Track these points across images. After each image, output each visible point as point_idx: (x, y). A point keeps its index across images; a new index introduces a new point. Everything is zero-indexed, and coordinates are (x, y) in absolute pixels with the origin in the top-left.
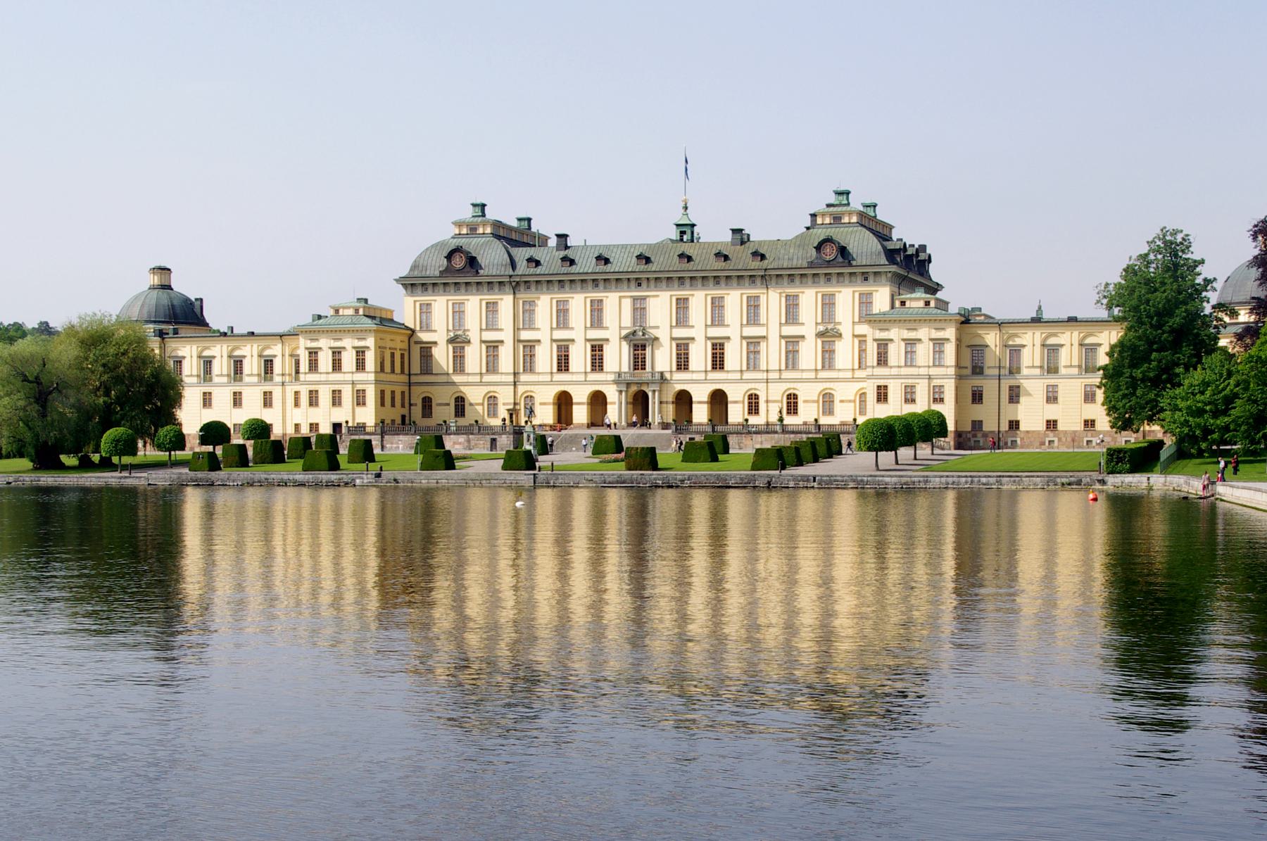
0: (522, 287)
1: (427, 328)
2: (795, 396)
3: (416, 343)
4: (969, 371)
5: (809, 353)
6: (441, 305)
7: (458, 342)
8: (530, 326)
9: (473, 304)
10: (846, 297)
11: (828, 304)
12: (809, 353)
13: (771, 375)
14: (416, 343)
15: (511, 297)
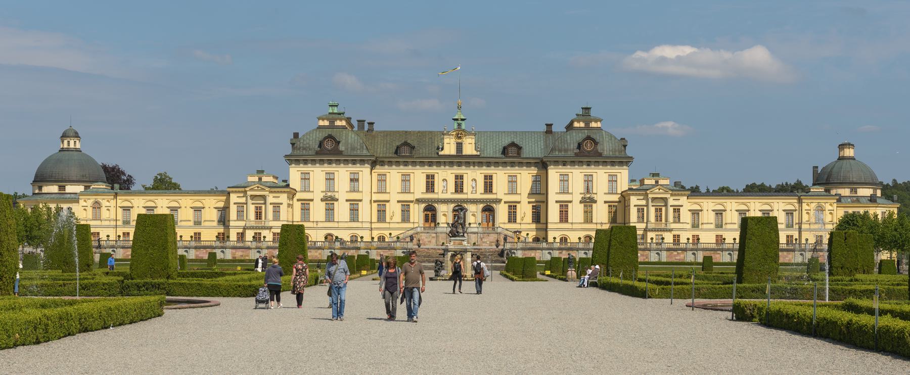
0: (378, 167)
1: (306, 189)
2: (566, 239)
3: (298, 200)
4: (689, 226)
5: (576, 212)
6: (318, 173)
7: (330, 200)
8: (382, 191)
9: (343, 173)
10: (601, 175)
11: (588, 180)
12: (576, 212)
13: (550, 226)
14: (298, 200)
15: (369, 170)
